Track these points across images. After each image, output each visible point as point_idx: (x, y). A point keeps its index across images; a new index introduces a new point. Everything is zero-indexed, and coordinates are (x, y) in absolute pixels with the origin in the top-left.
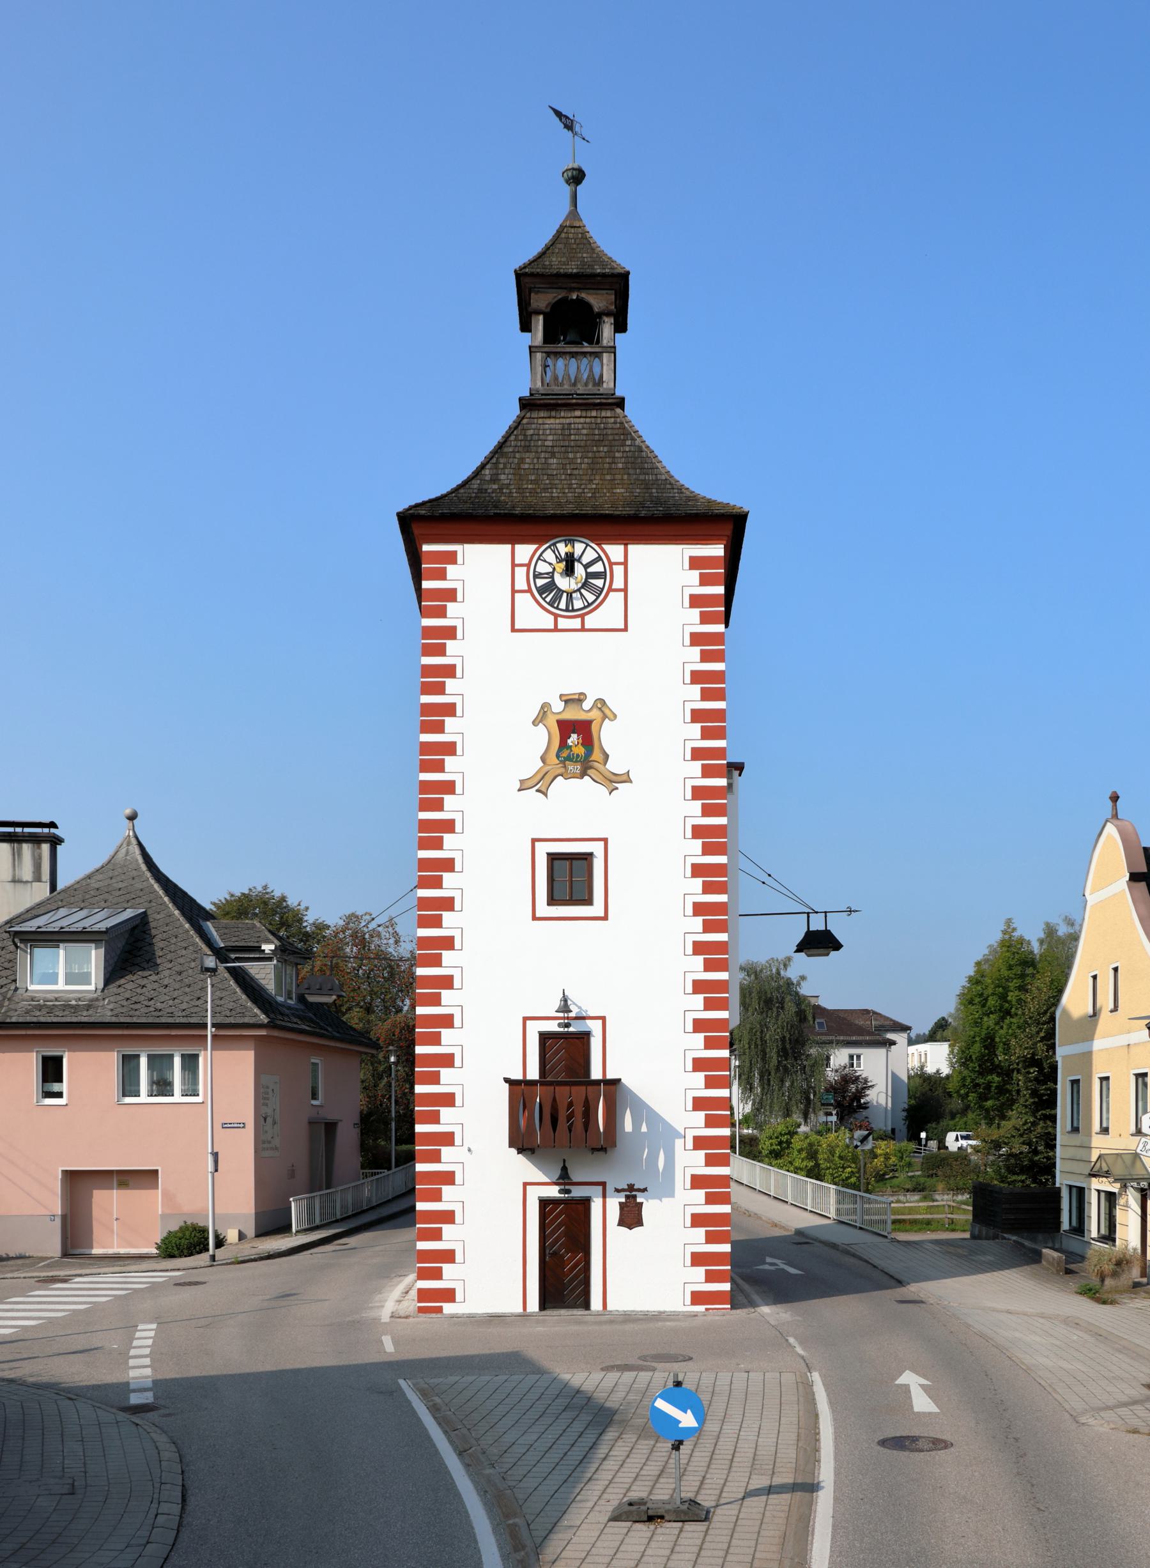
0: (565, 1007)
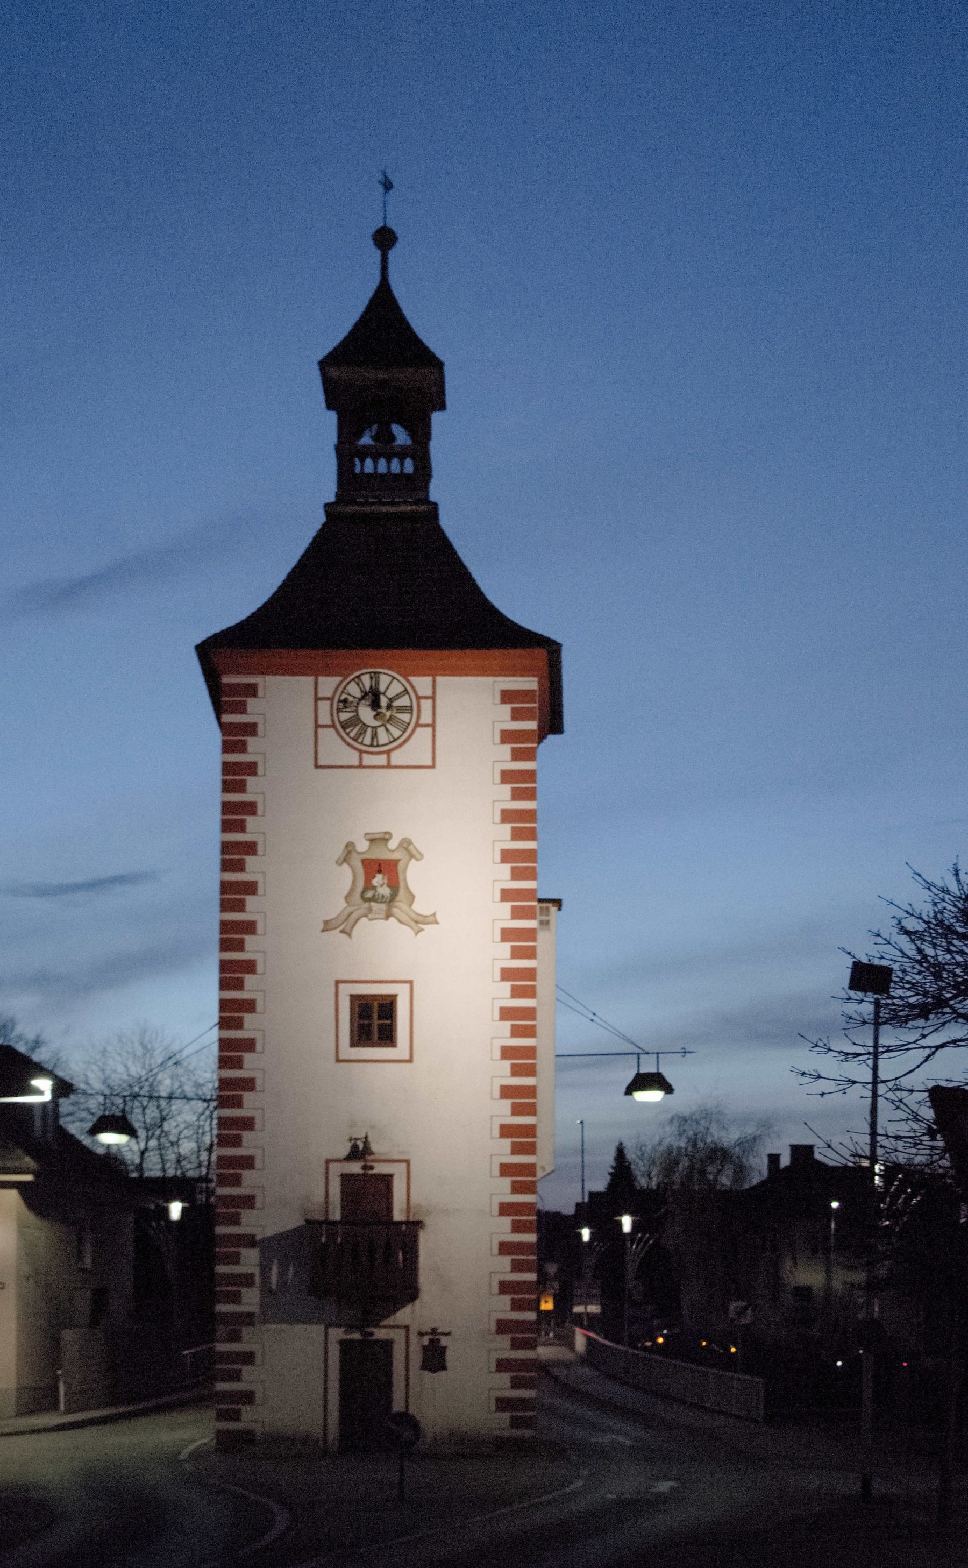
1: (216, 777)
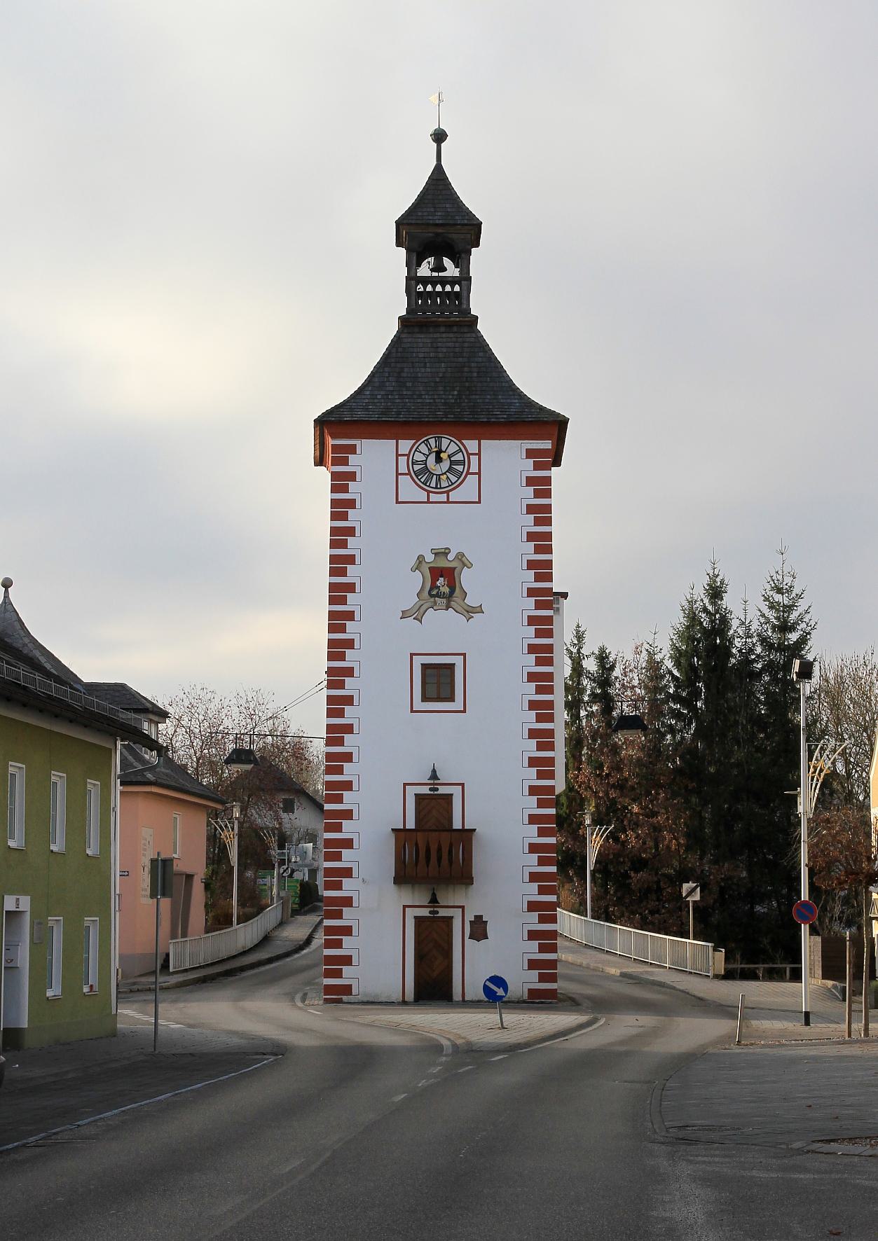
0: (434, 776)
1: (327, 510)
